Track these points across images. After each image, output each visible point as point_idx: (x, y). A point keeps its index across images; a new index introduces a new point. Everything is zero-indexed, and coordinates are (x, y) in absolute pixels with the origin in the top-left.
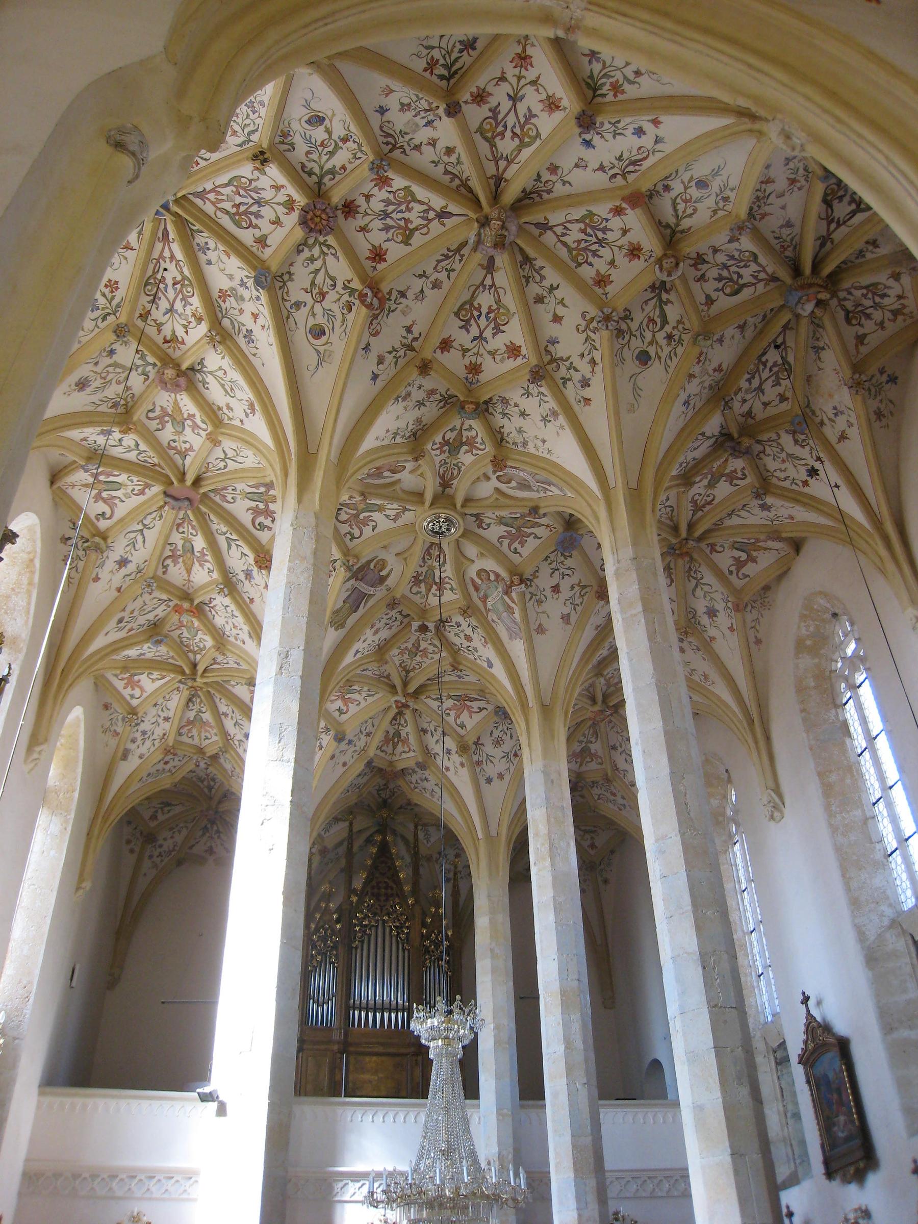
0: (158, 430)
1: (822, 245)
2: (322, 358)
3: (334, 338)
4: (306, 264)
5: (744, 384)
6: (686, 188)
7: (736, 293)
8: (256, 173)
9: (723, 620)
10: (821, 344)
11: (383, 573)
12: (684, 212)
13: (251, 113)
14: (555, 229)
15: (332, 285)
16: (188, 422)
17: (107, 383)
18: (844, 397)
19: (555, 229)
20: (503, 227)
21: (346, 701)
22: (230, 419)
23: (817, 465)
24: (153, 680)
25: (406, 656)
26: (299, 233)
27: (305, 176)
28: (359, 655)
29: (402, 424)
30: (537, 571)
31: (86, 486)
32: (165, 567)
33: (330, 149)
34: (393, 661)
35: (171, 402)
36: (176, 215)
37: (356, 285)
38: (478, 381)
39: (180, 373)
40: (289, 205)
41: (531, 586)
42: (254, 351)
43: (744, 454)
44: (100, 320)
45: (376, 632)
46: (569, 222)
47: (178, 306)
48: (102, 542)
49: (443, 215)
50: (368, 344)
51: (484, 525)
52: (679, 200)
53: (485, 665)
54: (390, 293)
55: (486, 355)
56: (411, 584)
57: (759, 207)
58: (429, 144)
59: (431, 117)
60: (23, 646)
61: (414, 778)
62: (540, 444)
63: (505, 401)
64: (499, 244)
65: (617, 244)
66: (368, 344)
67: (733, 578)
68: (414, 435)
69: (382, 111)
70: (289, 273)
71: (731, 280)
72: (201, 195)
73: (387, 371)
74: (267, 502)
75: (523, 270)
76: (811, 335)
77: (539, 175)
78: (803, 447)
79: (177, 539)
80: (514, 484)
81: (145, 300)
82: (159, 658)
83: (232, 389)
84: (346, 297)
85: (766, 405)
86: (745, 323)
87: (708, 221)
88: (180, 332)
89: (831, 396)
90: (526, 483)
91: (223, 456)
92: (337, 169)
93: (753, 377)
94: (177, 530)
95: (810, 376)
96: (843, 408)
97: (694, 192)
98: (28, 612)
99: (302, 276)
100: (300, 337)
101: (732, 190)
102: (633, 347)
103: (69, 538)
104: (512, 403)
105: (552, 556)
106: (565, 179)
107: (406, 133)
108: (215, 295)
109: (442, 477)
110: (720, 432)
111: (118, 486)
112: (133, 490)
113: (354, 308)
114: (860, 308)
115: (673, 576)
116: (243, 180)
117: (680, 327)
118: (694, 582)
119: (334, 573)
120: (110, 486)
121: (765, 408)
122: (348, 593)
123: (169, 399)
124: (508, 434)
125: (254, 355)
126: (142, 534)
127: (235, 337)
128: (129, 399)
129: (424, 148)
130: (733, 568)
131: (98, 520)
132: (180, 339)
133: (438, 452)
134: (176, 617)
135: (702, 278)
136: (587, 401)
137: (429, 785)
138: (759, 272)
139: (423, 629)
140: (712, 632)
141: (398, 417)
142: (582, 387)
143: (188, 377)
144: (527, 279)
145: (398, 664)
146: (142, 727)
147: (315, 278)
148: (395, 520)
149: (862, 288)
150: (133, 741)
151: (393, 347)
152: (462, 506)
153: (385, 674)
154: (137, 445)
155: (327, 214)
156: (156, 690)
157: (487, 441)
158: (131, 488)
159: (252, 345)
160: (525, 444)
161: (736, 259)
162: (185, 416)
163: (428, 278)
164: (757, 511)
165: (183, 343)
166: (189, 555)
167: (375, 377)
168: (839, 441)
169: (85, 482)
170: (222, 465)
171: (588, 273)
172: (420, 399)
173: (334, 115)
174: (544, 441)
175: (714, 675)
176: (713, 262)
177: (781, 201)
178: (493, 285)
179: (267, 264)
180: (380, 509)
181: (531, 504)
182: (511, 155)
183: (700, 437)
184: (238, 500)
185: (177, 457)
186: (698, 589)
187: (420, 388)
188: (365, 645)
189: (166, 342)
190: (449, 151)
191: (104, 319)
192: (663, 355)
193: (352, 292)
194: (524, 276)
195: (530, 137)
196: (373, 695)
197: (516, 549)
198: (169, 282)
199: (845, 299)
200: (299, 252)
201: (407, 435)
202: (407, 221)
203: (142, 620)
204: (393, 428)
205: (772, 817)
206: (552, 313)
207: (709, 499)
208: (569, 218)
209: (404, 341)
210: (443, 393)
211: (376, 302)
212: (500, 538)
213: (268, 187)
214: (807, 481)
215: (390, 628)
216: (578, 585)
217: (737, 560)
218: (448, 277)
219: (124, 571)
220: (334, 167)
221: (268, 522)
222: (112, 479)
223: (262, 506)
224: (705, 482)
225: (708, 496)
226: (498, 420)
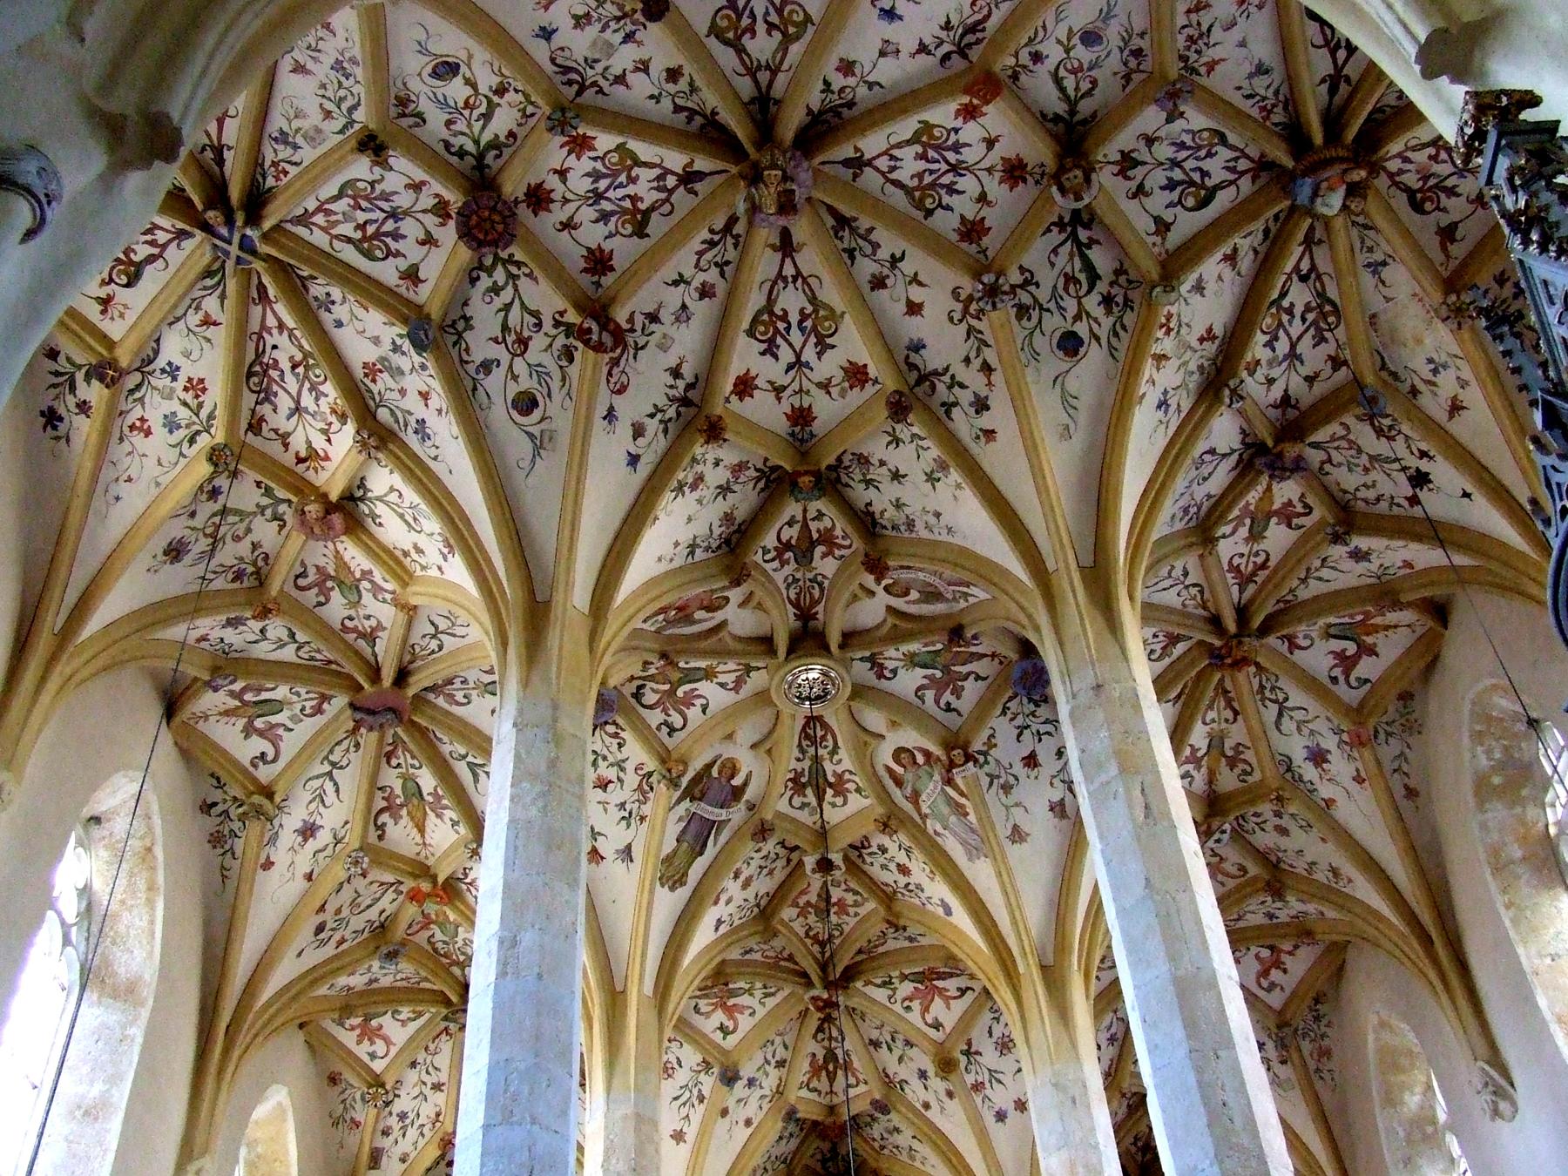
0: (320, 604)
1: (1333, 91)
2: (539, 444)
3: (553, 408)
4: (488, 299)
5: (1262, 354)
6: (1067, 51)
7: (1203, 204)
8: (377, 169)
9: (1340, 766)
10: (1378, 256)
11: (737, 781)
12: (1077, 89)
13: (343, 79)
14: (877, 163)
15: (535, 325)
16: (365, 584)
19: (877, 163)
20: (786, 178)
21: (730, 1011)
22: (423, 568)
23: (1424, 465)
24: (404, 1023)
25: (812, 918)
26: (465, 254)
27: (454, 160)
28: (723, 929)
29: (699, 528)
30: (992, 736)
31: (227, 713)
32: (381, 828)
33: (483, 109)
34: (791, 930)
36: (268, 258)
37: (572, 317)
38: (812, 435)
39: (330, 508)
40: (441, 209)
41: (987, 762)
42: (433, 452)
43: (1292, 471)
44: (186, 444)
45: (746, 885)
46: (899, 146)
47: (307, 400)
48: (266, 802)
49: (689, 178)
50: (611, 409)
51: (887, 673)
52: (1062, 73)
53: (940, 911)
54: (631, 320)
55: (814, 390)
56: (789, 793)
57: (1198, 52)
58: (637, 69)
59: (630, 28)
60: (148, 993)
61: (876, 1131)
62: (932, 520)
63: (863, 460)
64: (787, 205)
65: (986, 164)
66: (611, 409)
67: (1341, 689)
68: (727, 542)
69: (546, 34)
70: (467, 319)
71: (1192, 183)
72: (304, 220)
73: (653, 446)
75: (841, 239)
76: (1357, 245)
77: (827, 83)
79: (391, 778)
80: (914, 595)
81: (249, 399)
82: (404, 983)
83: (415, 519)
84: (561, 340)
85: (1310, 380)
86: (1235, 250)
87: (1122, 95)
88: (319, 443)
89: (1419, 341)
91: (432, 631)
92: (502, 139)
93: (1276, 339)
94: (388, 763)
95: (1374, 316)
97: (1082, 54)
98: (153, 934)
99: (485, 316)
100: (499, 415)
101: (1142, 35)
102: (1048, 331)
103: (215, 804)
105: (1013, 705)
106: (870, 78)
107: (596, 61)
108: (359, 373)
109: (796, 605)
110: (1243, 442)
111: (276, 706)
113: (577, 355)
114: (1432, 182)
115: (1235, 705)
116: (361, 185)
117: (1122, 279)
118: (1274, 708)
119: (651, 795)
120: (266, 708)
121: (1311, 387)
123: (326, 551)
124: (882, 513)
125: (435, 458)
126: (332, 779)
127: (402, 435)
128: (260, 563)
129: (630, 78)
130: (1337, 672)
131: (255, 766)
132: (322, 454)
133: (776, 564)
134: (412, 910)
135: (1140, 192)
136: (989, 434)
137: (904, 1139)
138: (1236, 159)
139: (825, 865)
140: (1325, 791)
141: (690, 520)
142: (977, 412)
143: (348, 512)
144: (851, 253)
145: (802, 934)
146: (398, 1106)
147: (506, 316)
148: (736, 689)
149: (1425, 146)
150: (386, 1133)
151: (655, 406)
152: (842, 647)
153: (785, 955)
154: (292, 635)
155: (500, 213)
156: (411, 1039)
157: (849, 530)
158: (299, 707)
159: (429, 443)
160: (910, 525)
161: (1189, 148)
162: (358, 575)
163: (688, 283)
164: (1348, 564)
165: (327, 458)
166: (415, 801)
167: (634, 460)
168: (1451, 417)
169: (222, 708)
170: (434, 644)
171: (946, 223)
172: (723, 482)
173: (470, 57)
174: (938, 515)
175: (1348, 869)
176: (1148, 159)
177: (1236, 34)
178: (798, 274)
179: (426, 310)
180: (709, 674)
181: (951, 624)
182: (774, 57)
183: (1207, 457)
185: (361, 643)
186: (1285, 720)
187: (717, 464)
188: (732, 908)
189: (300, 461)
190: (673, 74)
191: (192, 441)
192: (1103, 333)
193: (569, 330)
194: (844, 250)
195: (795, 24)
196: (773, 994)
197: (948, 704)
198: (285, 365)
199: (1401, 172)
200: (474, 281)
202: (634, 199)
203: (358, 922)
204: (685, 537)
205: (1496, 1113)
206: (904, 301)
207: (1259, 560)
208: (893, 141)
209: (672, 392)
211: (607, 339)
212: (919, 689)
213: (401, 189)
215: (771, 873)
217: (1340, 656)
218: (722, 274)
219: (312, 845)
220: (497, 136)
222: (265, 696)
224: (1243, 532)
225: (1257, 554)
226: (860, 495)
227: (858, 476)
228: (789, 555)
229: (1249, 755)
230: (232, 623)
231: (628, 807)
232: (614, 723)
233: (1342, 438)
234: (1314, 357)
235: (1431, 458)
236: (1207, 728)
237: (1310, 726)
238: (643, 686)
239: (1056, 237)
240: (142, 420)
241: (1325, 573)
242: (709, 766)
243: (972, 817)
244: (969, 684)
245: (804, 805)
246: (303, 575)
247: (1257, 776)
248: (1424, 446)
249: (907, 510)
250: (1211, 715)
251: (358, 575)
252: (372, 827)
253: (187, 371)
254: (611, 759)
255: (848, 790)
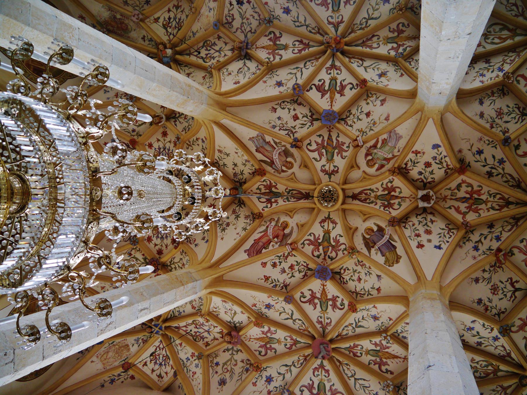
0: (275, 352)
11: (375, 229)
17: (232, 372)
18: (204, 11)
30: (359, 130)
32: (387, 371)
33: (135, 260)
35: (256, 341)
41: (366, 132)
47: (206, 328)
51: (336, 169)
52: (137, 124)
56: (391, 210)
63: (235, 174)
65: (163, 141)
74: (327, 299)
78: (233, 15)
80: (289, 159)
85: (226, 44)
89: (207, 16)
90: (282, 154)
96: (207, 8)
104: (234, 171)
105: (350, 123)
109: (300, 199)
112: (325, 376)
114: (177, 26)
118: (370, 22)
119: (364, 262)
122: (379, 253)
124: (251, 170)
126: (358, 379)
128: (249, 362)
133: (274, 205)
149: (167, 31)
154: (286, 366)
158: (324, 377)
160: (246, 161)
162: (265, 336)
164: (294, 13)
166: (380, 354)
184: (329, 316)
185: (298, 345)
186: (374, 16)
197: (347, 147)
198: (196, 330)
201: (252, 222)
204: (239, 230)
207: (297, 43)
210: (236, 205)
212: (342, 158)
214: (247, 2)
216: (366, 100)
218: (185, 209)
221: (339, 300)
222: (316, 386)
223: (330, 303)
224: (282, 52)
225: (295, 45)
226: (246, 175)
227: (241, 177)
228: (273, 200)
229: (394, 26)
230: (269, 380)
231: (366, 272)
232: (340, 269)
233: (241, 29)
234: (220, 44)
235: (231, 2)
236: (382, 46)
237: (374, 6)
238: (329, 257)
239: (177, 123)
240: (193, 373)
241: (301, 19)
242: (364, 238)
243: (385, 136)
244: (340, 139)
245: (400, 204)
246: (260, 353)
247: (402, 20)
248: (229, 6)
249: (244, 162)
250: (375, 45)
251: (265, 336)
252: (385, 374)
253: (189, 355)
254: (352, 274)
255: (392, 186)
